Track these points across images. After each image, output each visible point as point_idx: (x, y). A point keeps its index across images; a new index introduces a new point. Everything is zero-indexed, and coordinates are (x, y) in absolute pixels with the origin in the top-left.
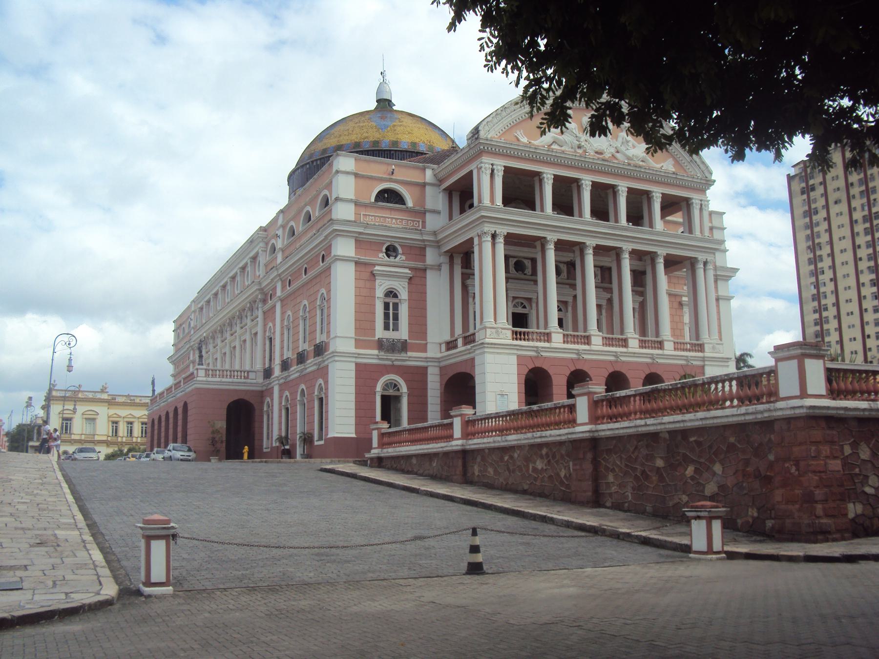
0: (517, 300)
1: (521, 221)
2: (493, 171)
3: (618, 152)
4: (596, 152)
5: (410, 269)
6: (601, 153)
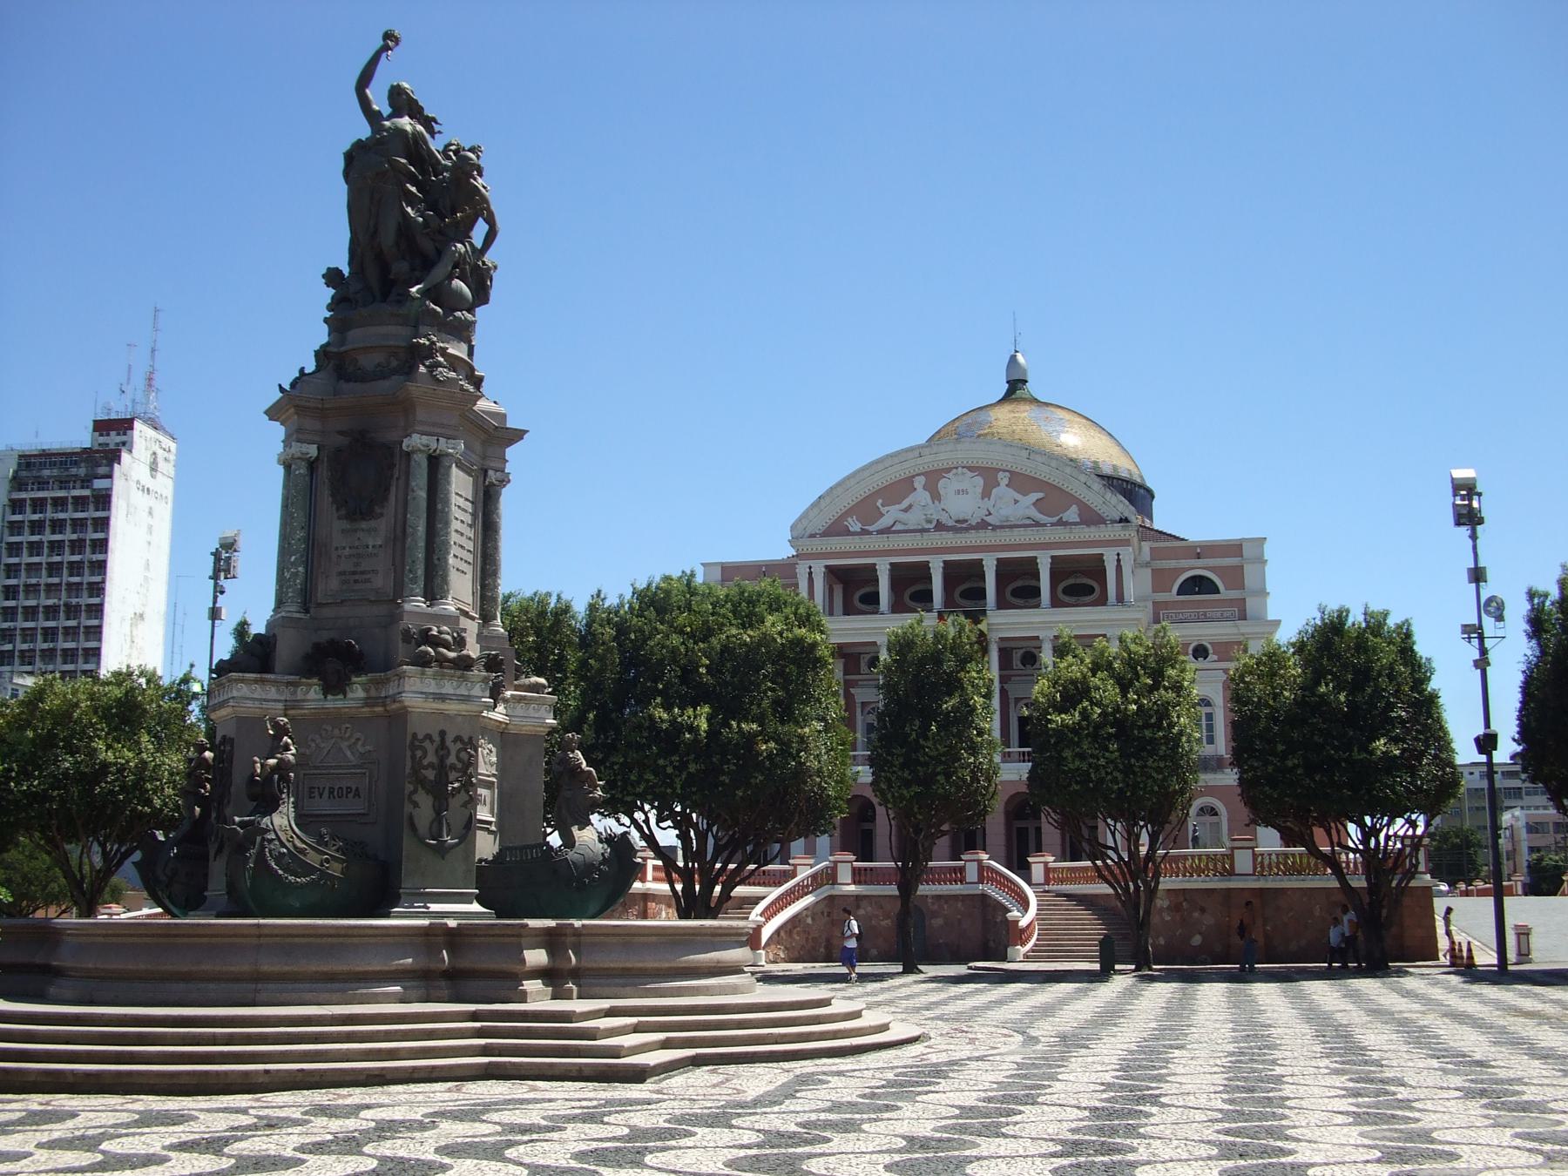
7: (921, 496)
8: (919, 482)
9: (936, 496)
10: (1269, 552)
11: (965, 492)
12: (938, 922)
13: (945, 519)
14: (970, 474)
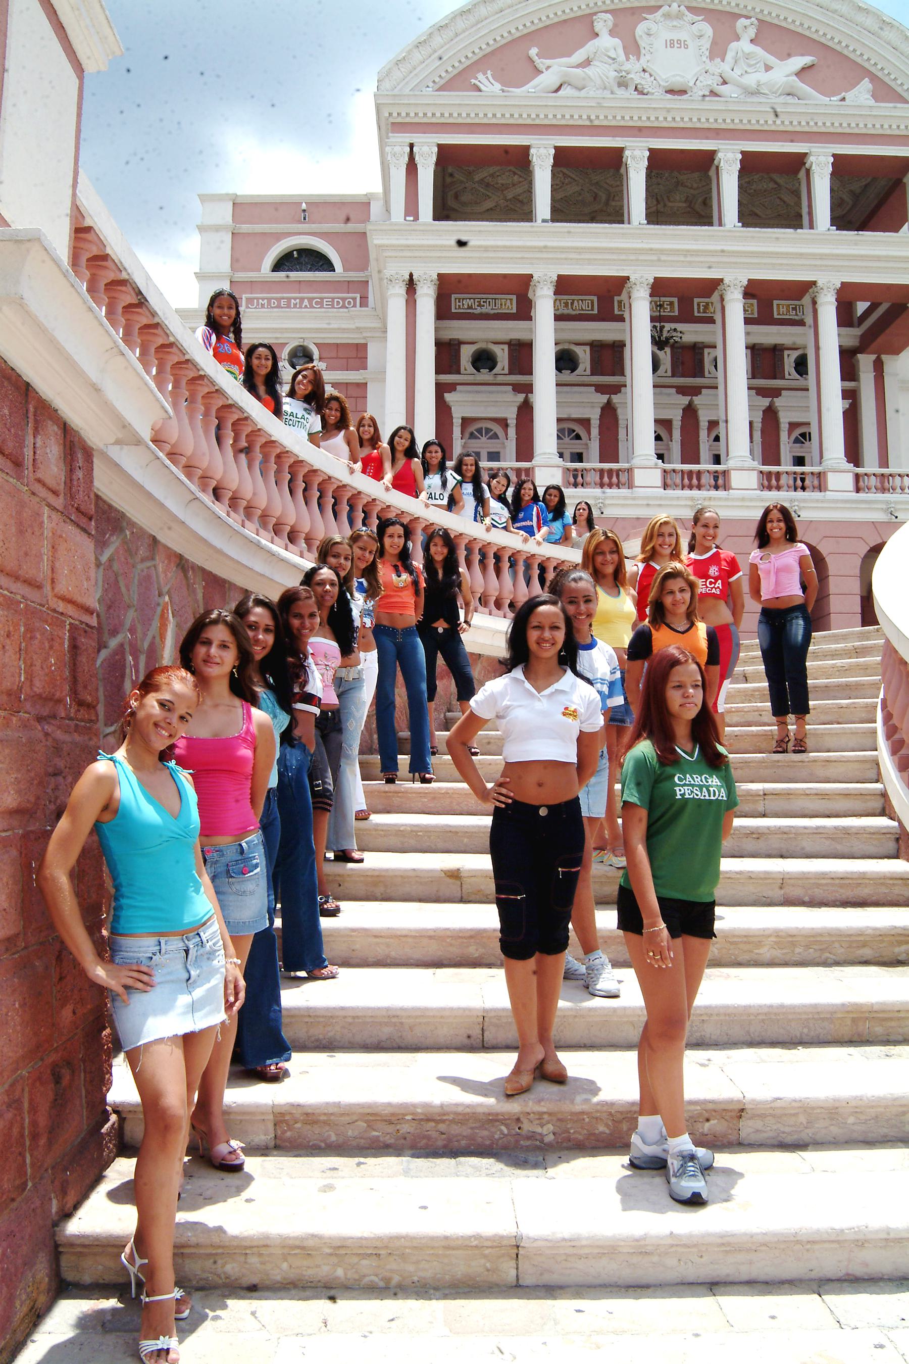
3: (725, 83)
4: (670, 91)
6: (683, 92)
7: (607, 43)
8: (603, 23)
9: (633, 48)
13: (646, 82)
14: (689, 16)
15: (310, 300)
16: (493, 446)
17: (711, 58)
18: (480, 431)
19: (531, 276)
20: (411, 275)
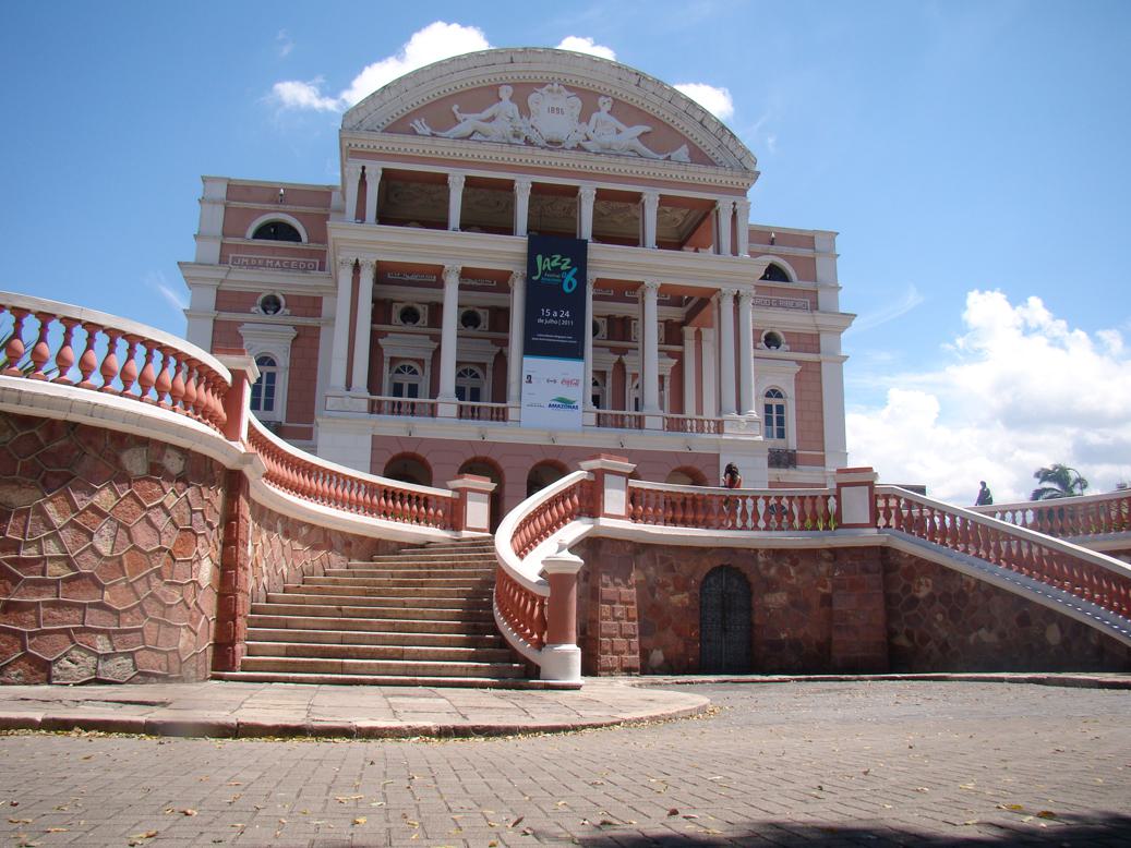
0: (466, 367)
1: (410, 245)
2: (363, 175)
3: (588, 139)
5: (295, 327)
8: (505, 93)
9: (525, 111)
10: (840, 245)
11: (559, 111)
12: (778, 599)
13: (533, 136)
14: (567, 93)
15: (281, 262)
16: (413, 379)
17: (580, 121)
18: (403, 367)
19: (443, 267)
20: (357, 260)
